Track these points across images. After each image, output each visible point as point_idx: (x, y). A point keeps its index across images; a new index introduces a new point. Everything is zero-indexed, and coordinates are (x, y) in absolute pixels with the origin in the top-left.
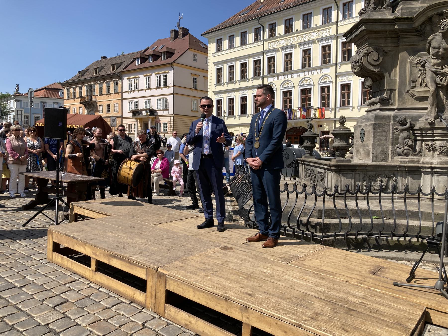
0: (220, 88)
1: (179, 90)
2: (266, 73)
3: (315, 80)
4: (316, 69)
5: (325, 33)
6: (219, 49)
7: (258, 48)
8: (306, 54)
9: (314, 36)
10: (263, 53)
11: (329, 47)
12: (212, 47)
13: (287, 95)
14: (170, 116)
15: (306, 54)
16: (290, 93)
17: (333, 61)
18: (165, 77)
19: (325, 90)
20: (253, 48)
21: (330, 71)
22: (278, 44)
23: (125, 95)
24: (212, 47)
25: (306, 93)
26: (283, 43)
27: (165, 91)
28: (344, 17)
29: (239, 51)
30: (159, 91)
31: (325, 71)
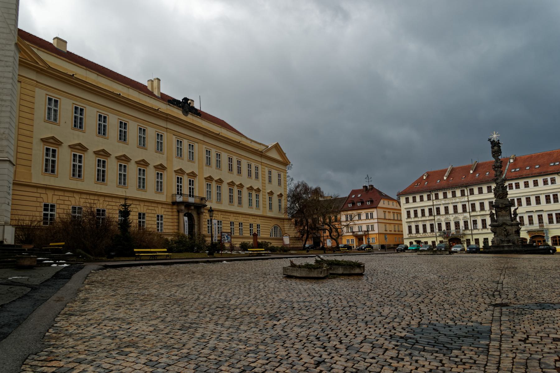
0: (409, 220)
1: (380, 221)
2: (436, 214)
3: (461, 218)
4: (461, 213)
5: (463, 200)
6: (407, 201)
7: (430, 203)
8: (455, 208)
9: (457, 200)
10: (433, 205)
11: (465, 205)
12: (403, 200)
13: (448, 224)
14: (376, 234)
15: (455, 208)
16: (449, 223)
17: (468, 211)
18: (372, 214)
19: (466, 223)
20: (427, 203)
21: (467, 215)
22: (441, 202)
23: (343, 223)
24: (403, 200)
25: (457, 224)
26: (443, 202)
27: (372, 221)
28: (471, 194)
29: (419, 204)
30: (368, 221)
31: (466, 214)
